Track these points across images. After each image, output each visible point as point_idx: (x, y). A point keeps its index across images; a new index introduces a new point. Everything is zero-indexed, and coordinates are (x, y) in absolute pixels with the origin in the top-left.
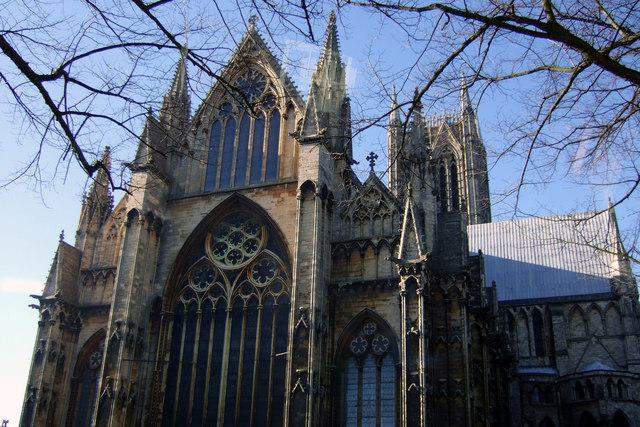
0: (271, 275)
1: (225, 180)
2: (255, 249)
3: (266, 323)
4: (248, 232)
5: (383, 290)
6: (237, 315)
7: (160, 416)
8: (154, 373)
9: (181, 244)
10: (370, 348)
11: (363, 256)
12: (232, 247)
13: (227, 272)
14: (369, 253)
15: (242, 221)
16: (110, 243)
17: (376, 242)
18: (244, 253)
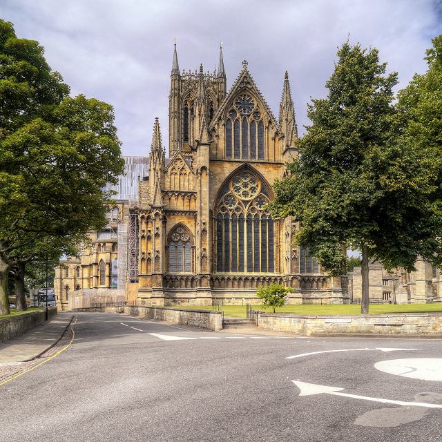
1: (237, 155)
3: (264, 225)
4: (251, 183)
6: (249, 222)
9: (218, 186)
13: (243, 201)
16: (173, 176)
18: (250, 193)
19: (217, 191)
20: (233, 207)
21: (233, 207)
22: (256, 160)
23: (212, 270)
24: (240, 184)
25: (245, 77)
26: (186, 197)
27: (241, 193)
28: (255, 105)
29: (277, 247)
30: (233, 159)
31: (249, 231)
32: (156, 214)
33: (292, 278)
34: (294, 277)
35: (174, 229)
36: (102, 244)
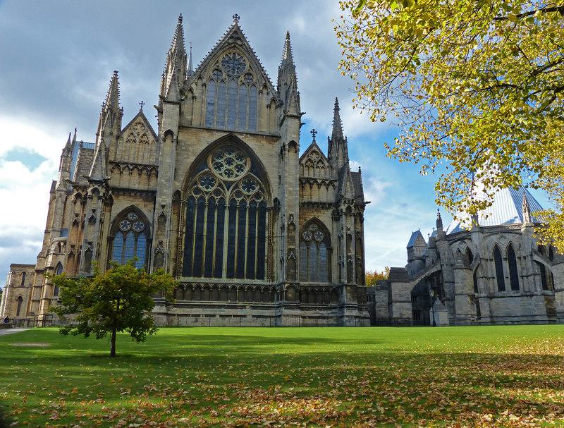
0: (254, 189)
2: (242, 171)
5: (323, 208)
6: (232, 209)
7: (182, 266)
8: (178, 239)
9: (192, 159)
10: (313, 237)
11: (311, 188)
12: (226, 166)
13: (225, 182)
14: (315, 186)
15: (233, 152)
17: (319, 181)
18: (235, 172)
19: (189, 166)
20: (211, 189)
21: (211, 189)
22: (247, 129)
23: (175, 274)
24: (223, 160)
25: (235, 32)
26: (145, 172)
27: (222, 171)
28: (248, 64)
29: (269, 244)
30: (214, 126)
31: (232, 222)
32: (94, 191)
33: (287, 288)
34: (291, 286)
35: (123, 215)
36: (62, 244)
